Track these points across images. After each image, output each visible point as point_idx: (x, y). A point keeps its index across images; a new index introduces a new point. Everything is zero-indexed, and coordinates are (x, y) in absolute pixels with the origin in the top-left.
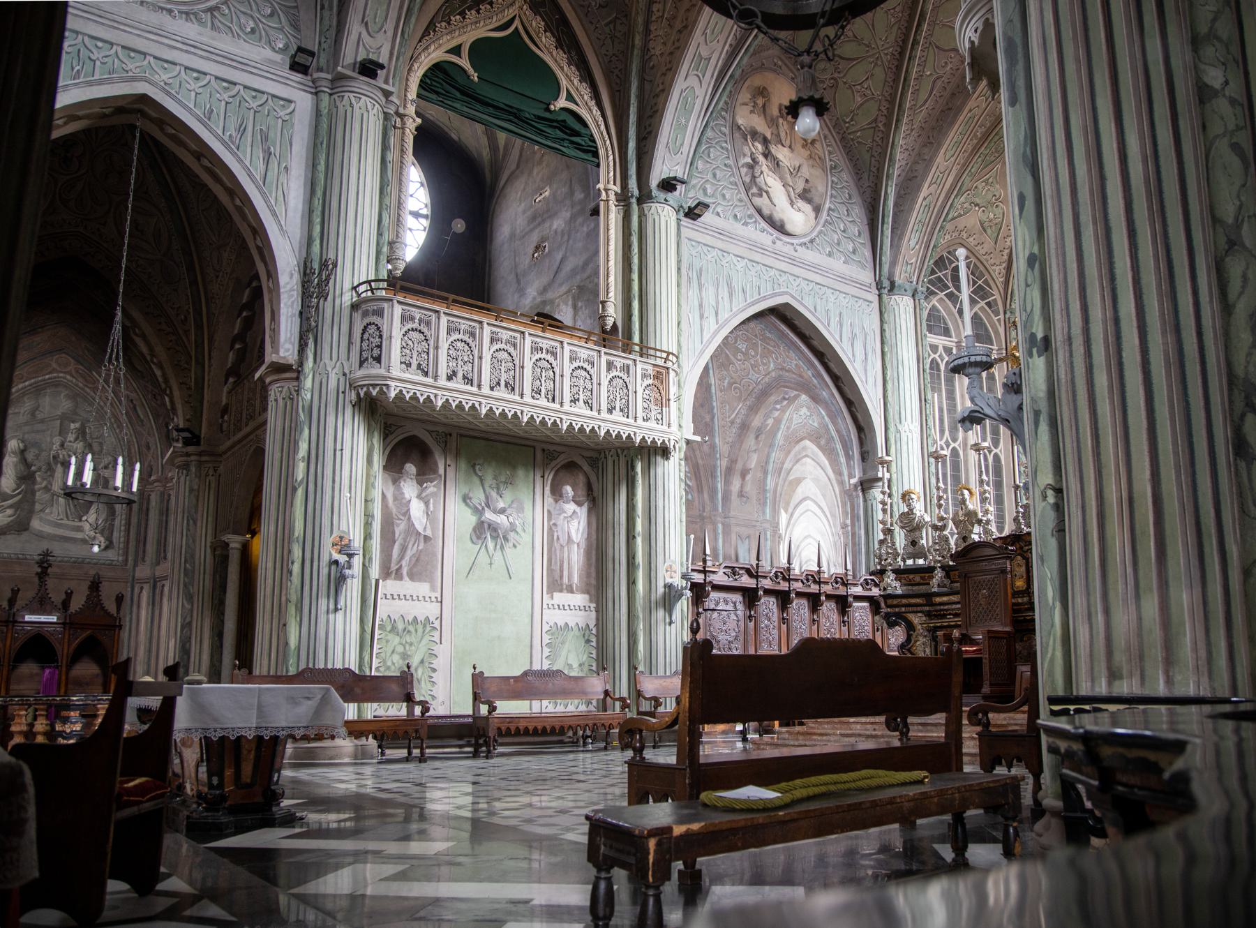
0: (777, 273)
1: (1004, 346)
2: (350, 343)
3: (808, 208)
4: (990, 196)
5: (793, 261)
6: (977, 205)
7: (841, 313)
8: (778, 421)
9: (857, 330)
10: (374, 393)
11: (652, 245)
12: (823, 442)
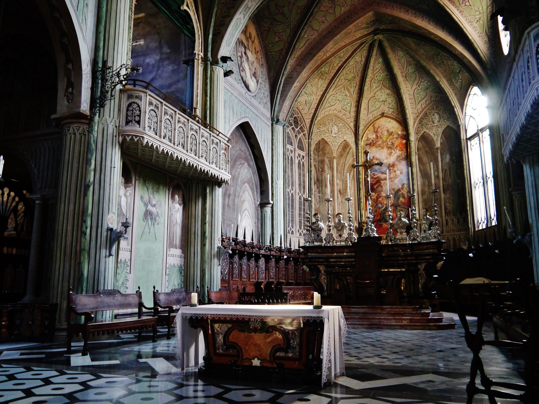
0: (246, 107)
2: (119, 110)
3: (255, 80)
4: (311, 91)
5: (250, 103)
6: (306, 93)
8: (239, 173)
9: (266, 138)
10: (136, 140)
11: (216, 86)
12: (251, 185)
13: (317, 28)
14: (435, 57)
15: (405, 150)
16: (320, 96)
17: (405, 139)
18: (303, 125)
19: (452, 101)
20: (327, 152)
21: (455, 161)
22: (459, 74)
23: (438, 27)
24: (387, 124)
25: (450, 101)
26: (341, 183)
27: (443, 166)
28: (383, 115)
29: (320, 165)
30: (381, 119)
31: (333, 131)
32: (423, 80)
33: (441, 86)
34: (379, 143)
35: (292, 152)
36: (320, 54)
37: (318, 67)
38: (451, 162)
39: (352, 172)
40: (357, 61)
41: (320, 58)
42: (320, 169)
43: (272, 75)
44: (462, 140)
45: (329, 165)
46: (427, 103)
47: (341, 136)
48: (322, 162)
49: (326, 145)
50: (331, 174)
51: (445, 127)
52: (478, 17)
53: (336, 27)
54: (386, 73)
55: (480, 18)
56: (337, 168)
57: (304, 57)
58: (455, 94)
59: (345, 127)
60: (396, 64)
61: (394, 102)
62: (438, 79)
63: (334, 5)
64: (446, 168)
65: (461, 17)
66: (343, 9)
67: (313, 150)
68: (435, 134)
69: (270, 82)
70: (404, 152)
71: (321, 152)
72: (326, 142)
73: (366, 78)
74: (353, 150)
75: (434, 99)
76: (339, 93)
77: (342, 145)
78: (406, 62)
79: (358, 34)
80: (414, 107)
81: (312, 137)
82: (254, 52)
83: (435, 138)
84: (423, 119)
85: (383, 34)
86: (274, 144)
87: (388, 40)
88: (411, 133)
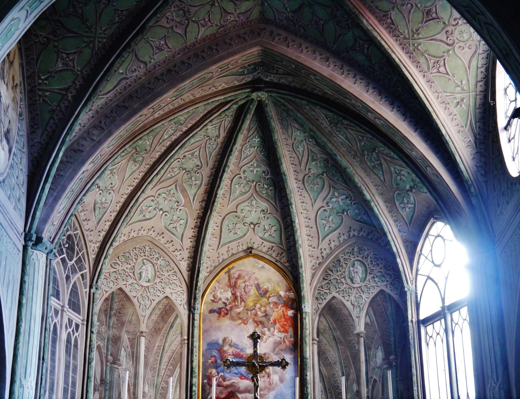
1: (86, 318)
4: (108, 183)
7: (6, 257)
9: (11, 278)
13: (146, 59)
14: (366, 153)
15: (291, 331)
16: (126, 196)
17: (292, 309)
18: (83, 254)
19: (392, 244)
20: (127, 318)
21: (394, 364)
22: (410, 193)
23: (383, 100)
24: (256, 271)
25: (388, 243)
26: (152, 392)
27: (370, 373)
28: (249, 252)
29: (110, 347)
30: (247, 261)
31: (143, 275)
33: (372, 209)
35: (56, 312)
36: (145, 111)
37: (133, 137)
38: (385, 366)
39: (178, 370)
40: (210, 134)
41: (143, 118)
42: (110, 358)
43: (38, 140)
44: (410, 324)
45: (129, 349)
46: (341, 240)
48: (116, 340)
49: (128, 305)
50: (133, 371)
51: (376, 291)
52: (459, 96)
53: (183, 63)
54: (264, 168)
55: (462, 100)
56: (145, 357)
57: (112, 111)
58: (399, 231)
59: (169, 268)
60: (287, 153)
61: (274, 228)
62: (368, 197)
63: (187, 19)
64: (374, 377)
65: (428, 90)
66: (203, 29)
67: (97, 312)
68: (356, 304)
69: (30, 154)
70: (288, 335)
71: (114, 319)
72: (127, 296)
73: (224, 171)
74: (182, 319)
75: (356, 234)
76: (163, 195)
77: (160, 306)
78: (306, 153)
79: (222, 85)
80: (315, 244)
82: (10, 86)
83: (354, 314)
84: (332, 271)
85: (270, 92)
86: (25, 292)
87: (276, 104)
88: (306, 296)
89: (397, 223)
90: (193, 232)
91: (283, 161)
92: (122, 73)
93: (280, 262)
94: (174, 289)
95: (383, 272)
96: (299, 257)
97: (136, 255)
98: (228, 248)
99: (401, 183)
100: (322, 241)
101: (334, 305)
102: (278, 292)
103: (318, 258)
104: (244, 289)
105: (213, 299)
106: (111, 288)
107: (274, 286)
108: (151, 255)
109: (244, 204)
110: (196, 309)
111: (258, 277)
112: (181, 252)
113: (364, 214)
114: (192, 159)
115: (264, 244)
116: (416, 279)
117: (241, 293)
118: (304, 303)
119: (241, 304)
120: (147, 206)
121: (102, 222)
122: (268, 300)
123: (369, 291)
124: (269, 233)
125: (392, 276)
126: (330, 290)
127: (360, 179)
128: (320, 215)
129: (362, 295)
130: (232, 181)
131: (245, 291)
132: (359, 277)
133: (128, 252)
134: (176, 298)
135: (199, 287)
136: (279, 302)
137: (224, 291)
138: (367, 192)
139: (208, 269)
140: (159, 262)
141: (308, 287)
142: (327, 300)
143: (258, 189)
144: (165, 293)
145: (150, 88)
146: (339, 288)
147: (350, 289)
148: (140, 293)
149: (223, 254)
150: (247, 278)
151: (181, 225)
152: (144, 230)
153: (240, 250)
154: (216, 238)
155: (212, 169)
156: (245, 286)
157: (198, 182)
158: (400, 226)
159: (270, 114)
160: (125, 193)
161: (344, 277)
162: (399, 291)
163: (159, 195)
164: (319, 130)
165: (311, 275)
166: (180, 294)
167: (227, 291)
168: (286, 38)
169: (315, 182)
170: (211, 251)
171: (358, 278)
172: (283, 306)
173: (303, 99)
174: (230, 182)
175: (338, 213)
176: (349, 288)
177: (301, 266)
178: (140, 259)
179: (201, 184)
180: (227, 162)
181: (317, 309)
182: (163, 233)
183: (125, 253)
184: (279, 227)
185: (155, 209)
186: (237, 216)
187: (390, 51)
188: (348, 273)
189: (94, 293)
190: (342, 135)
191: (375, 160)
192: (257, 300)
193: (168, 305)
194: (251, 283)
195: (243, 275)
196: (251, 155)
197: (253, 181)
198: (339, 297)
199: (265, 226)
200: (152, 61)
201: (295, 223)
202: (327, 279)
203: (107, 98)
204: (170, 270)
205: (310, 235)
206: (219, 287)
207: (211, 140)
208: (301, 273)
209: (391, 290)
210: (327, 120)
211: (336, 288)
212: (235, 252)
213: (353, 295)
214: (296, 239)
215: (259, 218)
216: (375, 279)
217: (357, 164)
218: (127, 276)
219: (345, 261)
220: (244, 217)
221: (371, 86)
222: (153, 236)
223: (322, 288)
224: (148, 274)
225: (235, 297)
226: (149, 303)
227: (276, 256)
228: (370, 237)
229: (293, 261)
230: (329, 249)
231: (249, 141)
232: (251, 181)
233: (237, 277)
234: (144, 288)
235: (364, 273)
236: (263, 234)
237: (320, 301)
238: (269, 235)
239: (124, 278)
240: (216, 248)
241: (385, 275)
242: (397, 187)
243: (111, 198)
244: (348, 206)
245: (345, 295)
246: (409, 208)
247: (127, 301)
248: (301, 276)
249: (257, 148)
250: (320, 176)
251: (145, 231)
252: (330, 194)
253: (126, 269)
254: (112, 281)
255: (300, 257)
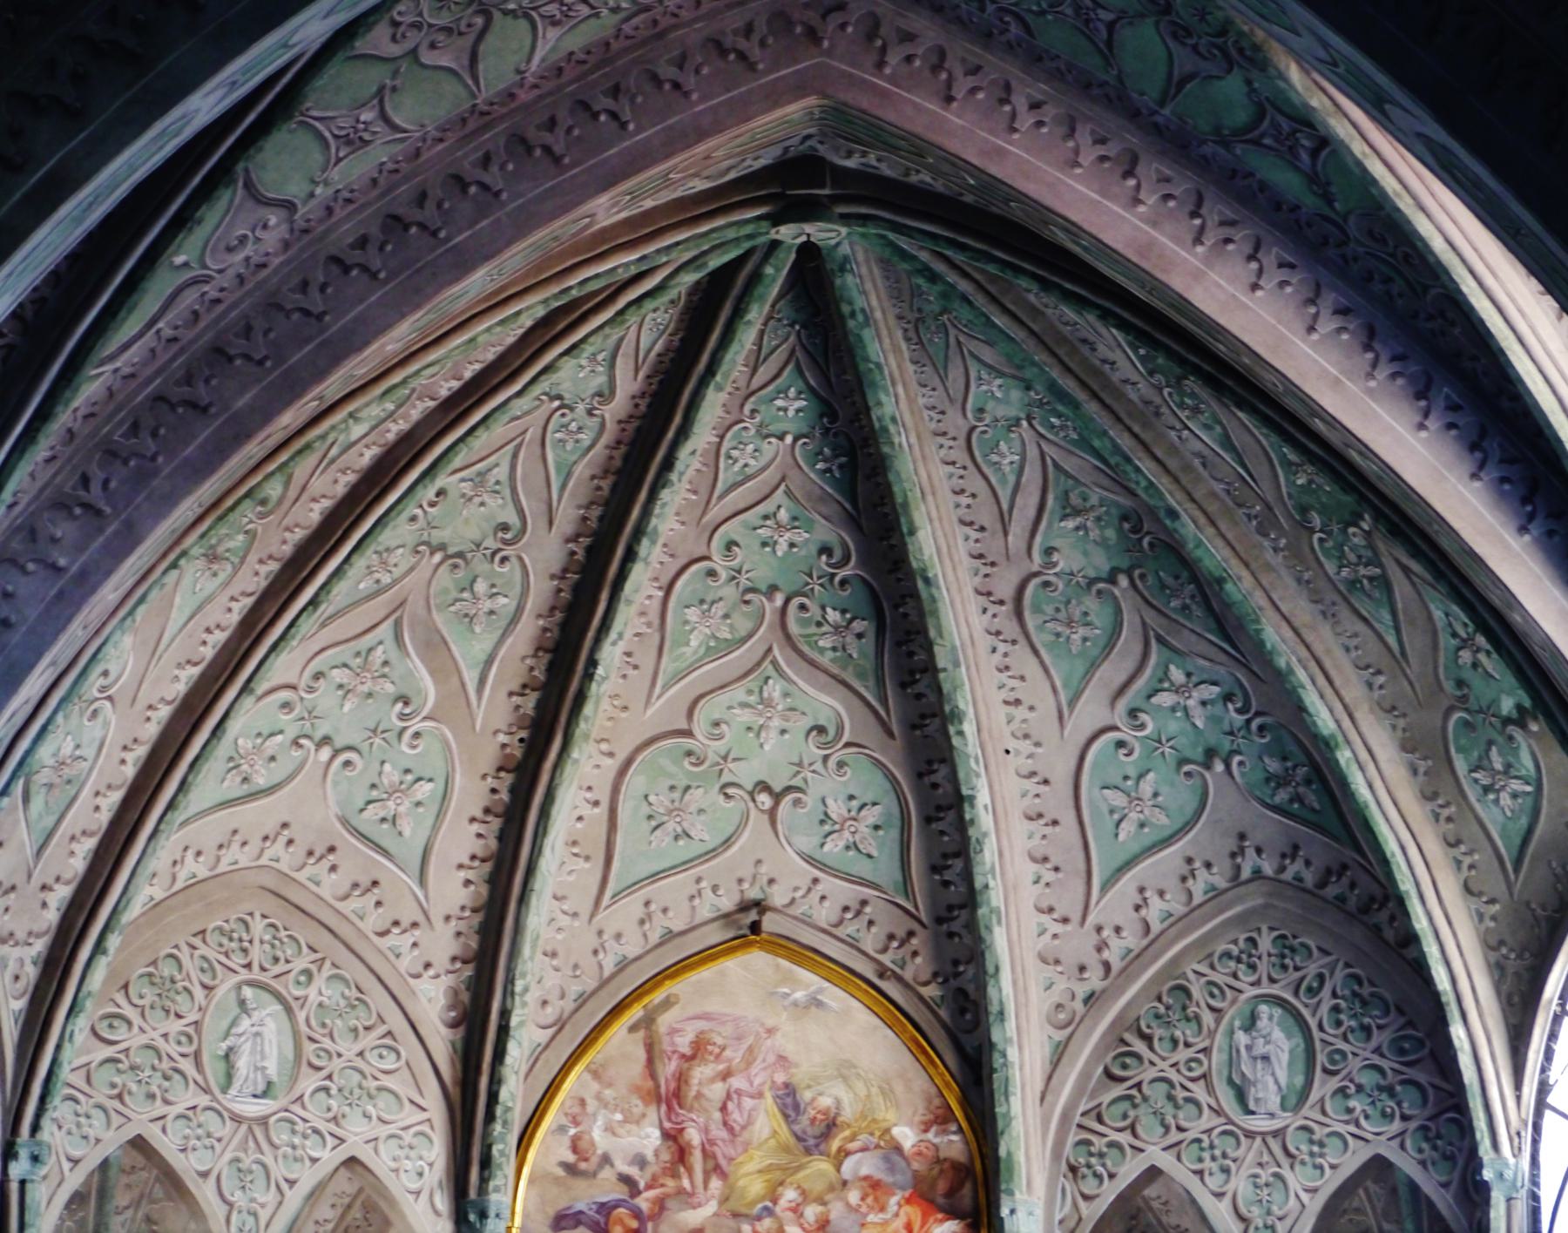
13: (294, 189)
14: (1316, 520)
16: (165, 712)
23: (1383, 373)
24: (782, 1020)
25: (1412, 939)
30: (732, 965)
31: (242, 1064)
32: (1177, 675)
34: (694, 1217)
46: (1198, 888)
47: (314, 1114)
53: (461, 183)
54: (825, 532)
57: (135, 428)
59: (360, 1018)
61: (871, 816)
62: (1324, 719)
66: (553, 34)
68: (1256, 1213)
72: (171, 1180)
73: (630, 556)
75: (1268, 869)
76: (338, 675)
77: (325, 1212)
78: (1032, 475)
80: (1069, 903)
81: (48, 1132)
84: (1148, 1039)
85: (864, 219)
88: (1020, 1157)
89: (1456, 852)
90: (479, 835)
91: (919, 515)
92: (186, 265)
93: (900, 979)
94: (386, 1117)
95: (1389, 1072)
96: (990, 969)
97: (208, 967)
98: (647, 904)
99: (1476, 680)
100: (1106, 887)
101: (1151, 1209)
102: (887, 1131)
103: (1082, 969)
104: (723, 1109)
105: (570, 1158)
106: (98, 1141)
107: (868, 1096)
108: (276, 960)
109: (723, 698)
110: (492, 1213)
111: (790, 1049)
112: (417, 933)
113: (1308, 782)
114: (477, 500)
115: (819, 887)
116: (1537, 1128)
117: (706, 1131)
118: (1011, 1193)
119: (706, 1187)
120: (259, 734)
121: (58, 845)
122: (838, 1170)
123: (1322, 1155)
124: (846, 834)
125: (1431, 1091)
126: (1135, 1135)
127: (1289, 634)
128: (1095, 764)
129: (1286, 1172)
130: (669, 590)
131: (725, 1124)
132: (1277, 1082)
133: (171, 956)
134: (393, 1165)
135: (508, 1109)
136: (887, 1178)
137: (626, 1121)
138: (1322, 696)
139: (549, 1010)
140: (312, 992)
141: (1030, 1112)
142: (1122, 1184)
143: (794, 628)
144: (342, 1141)
145: (306, 313)
146: (1180, 1129)
147: (1232, 1140)
148: (228, 1156)
149: (618, 936)
150: (735, 1055)
151: (418, 804)
152: (244, 844)
153: (705, 913)
154: (587, 858)
155: (574, 538)
156: (728, 1097)
157: (502, 600)
158: (1471, 867)
159: (860, 302)
160: (162, 699)
161: (1204, 1076)
162: (1456, 1175)
163: (318, 676)
164: (1095, 396)
165: (1047, 1051)
166: (415, 1141)
167: (638, 1122)
168: (942, 54)
169: (1077, 615)
170: (565, 921)
171: (1272, 1087)
172: (908, 1201)
173: (1018, 270)
174: (661, 594)
175: (1183, 761)
176: (1224, 1133)
177: (1001, 1013)
178: (226, 986)
179: (520, 609)
180: (646, 513)
181: (1072, 1224)
182: (332, 849)
183: (154, 963)
184: (896, 811)
185: (296, 743)
186: (689, 754)
187: (1405, 205)
188: (1225, 1056)
189: (23, 1183)
190: (1207, 427)
191: (1360, 557)
192: (783, 1169)
193: (358, 1203)
194: (757, 1082)
195: (719, 1041)
196: (763, 469)
197: (773, 589)
198: (1179, 1171)
199: (830, 802)
200: (318, 191)
201: (972, 806)
202: (1122, 1080)
203: (116, 371)
204: (367, 1028)
205: (1045, 859)
206: (598, 1097)
207: (572, 409)
208: (1000, 1047)
209: (1423, 1163)
210: (1136, 353)
211: (1167, 1129)
212: (677, 926)
213: (1245, 1172)
214: (978, 884)
215: (800, 764)
216: (1352, 1103)
217: (1277, 560)
218: (166, 1078)
219: (1212, 995)
220: (725, 758)
221: (1329, 299)
222: (283, 866)
223: (1100, 1120)
224: (263, 1058)
225: (681, 1154)
226: (271, 1197)
227: (880, 946)
228: (1331, 891)
229: (957, 975)
230: (1139, 927)
231: (753, 411)
232: (764, 588)
233: (687, 1050)
234: (244, 1127)
235: (1300, 1066)
236: (817, 840)
237: (1089, 1186)
238: (848, 848)
239: (154, 1089)
240: (585, 907)
241: (1398, 1088)
242: (1459, 693)
243: (98, 734)
244: (1231, 733)
245: (1208, 1164)
246: (1515, 796)
247: (170, 1199)
248: (997, 1061)
249: (796, 440)
250: (1101, 585)
251: (247, 848)
252: (1148, 672)
253: (160, 1043)
254: (99, 1106)
255: (997, 969)
